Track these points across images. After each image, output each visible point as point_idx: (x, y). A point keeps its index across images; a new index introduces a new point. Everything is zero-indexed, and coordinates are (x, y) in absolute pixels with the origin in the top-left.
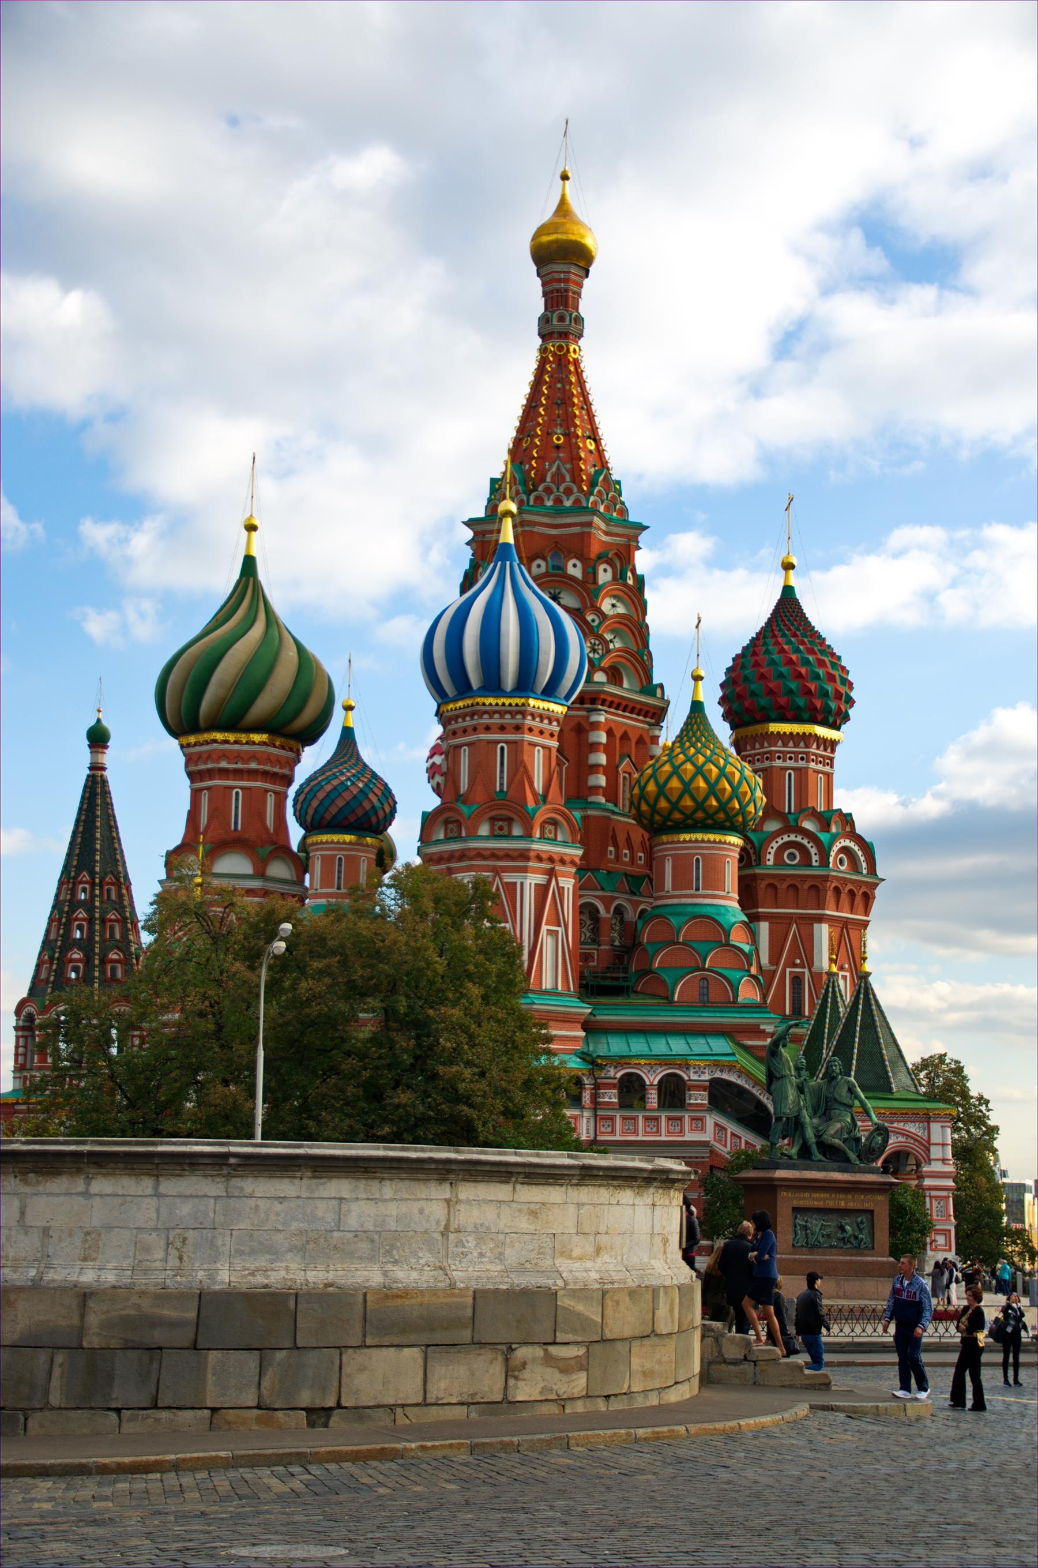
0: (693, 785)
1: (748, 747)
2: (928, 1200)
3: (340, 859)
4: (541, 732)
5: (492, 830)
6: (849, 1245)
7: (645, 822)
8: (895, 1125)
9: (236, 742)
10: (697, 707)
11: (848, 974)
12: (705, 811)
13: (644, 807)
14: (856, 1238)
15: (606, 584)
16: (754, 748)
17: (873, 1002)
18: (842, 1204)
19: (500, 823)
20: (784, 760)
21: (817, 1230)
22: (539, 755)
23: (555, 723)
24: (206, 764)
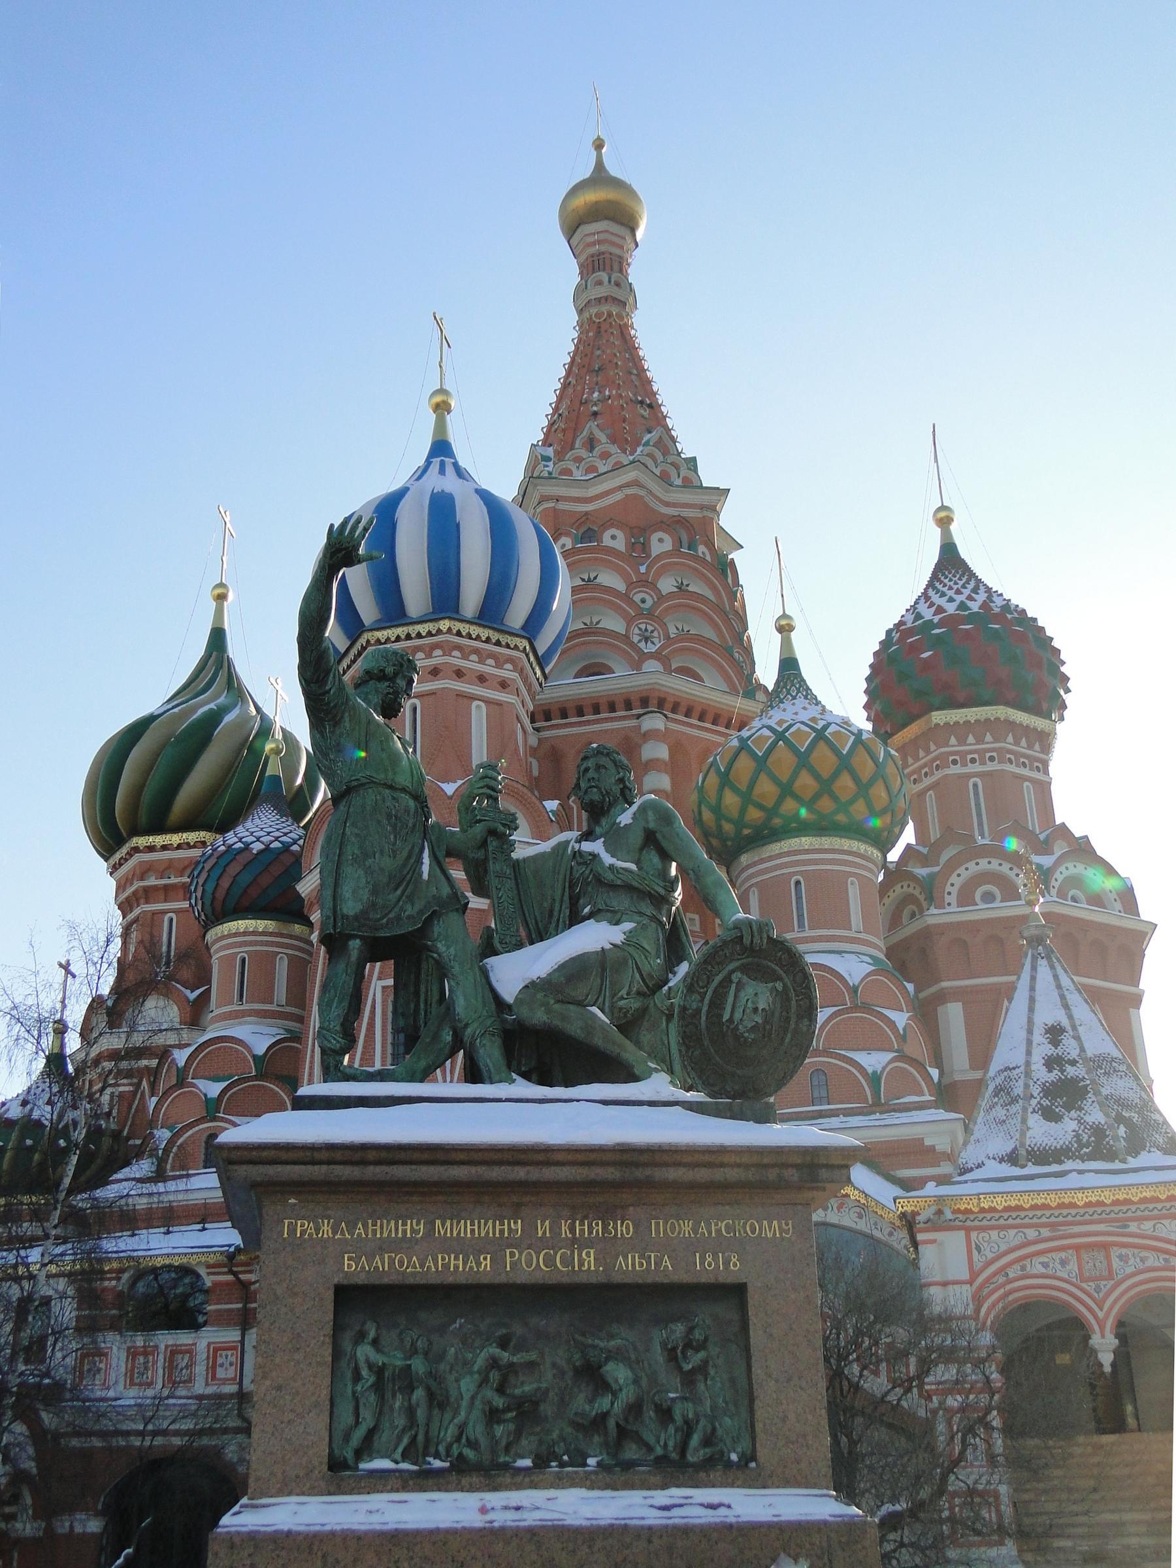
0: (770, 760)
1: (910, 760)
3: (243, 960)
4: (482, 679)
6: (631, 1452)
7: (715, 842)
8: (1133, 1227)
9: (164, 848)
10: (789, 665)
13: (707, 815)
14: (665, 1414)
15: (659, 557)
16: (917, 759)
18: (588, 1263)
20: (964, 765)
21: (467, 1385)
22: (479, 715)
23: (509, 666)
24: (132, 884)
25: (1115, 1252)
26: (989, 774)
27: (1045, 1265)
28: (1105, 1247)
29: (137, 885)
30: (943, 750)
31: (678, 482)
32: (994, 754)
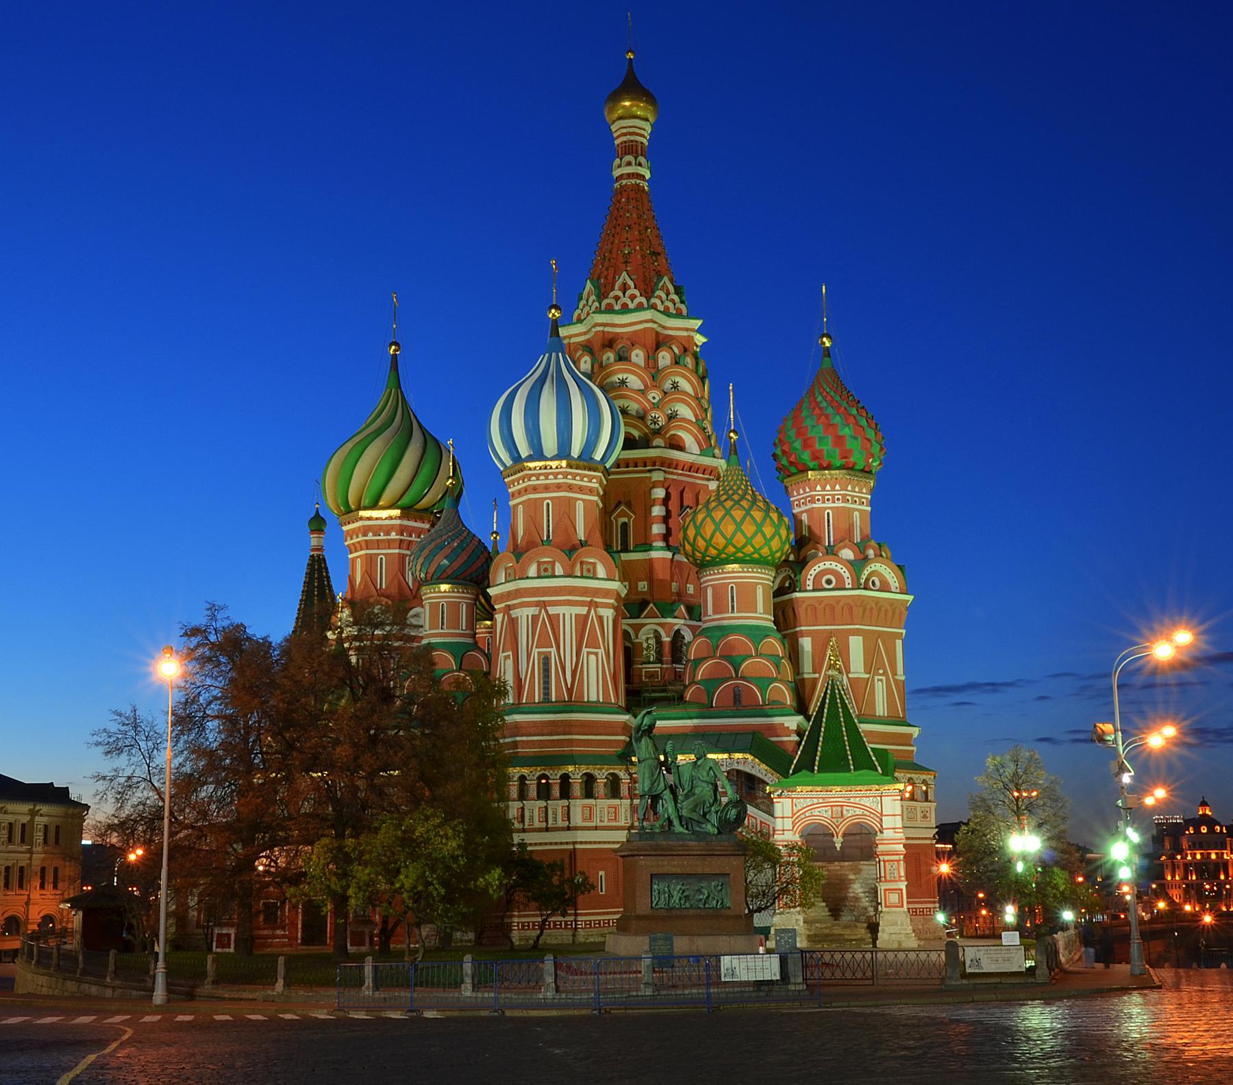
1: (795, 493)
2: (882, 863)
4: (581, 489)
5: (539, 570)
8: (852, 800)
9: (377, 519)
11: (884, 678)
12: (734, 547)
17: (838, 696)
18: (700, 870)
19: (546, 566)
20: (824, 502)
21: (675, 893)
23: (594, 480)
25: (845, 808)
26: (837, 508)
27: (819, 812)
28: (841, 806)
29: (361, 538)
30: (813, 493)
31: (674, 312)
32: (840, 497)
